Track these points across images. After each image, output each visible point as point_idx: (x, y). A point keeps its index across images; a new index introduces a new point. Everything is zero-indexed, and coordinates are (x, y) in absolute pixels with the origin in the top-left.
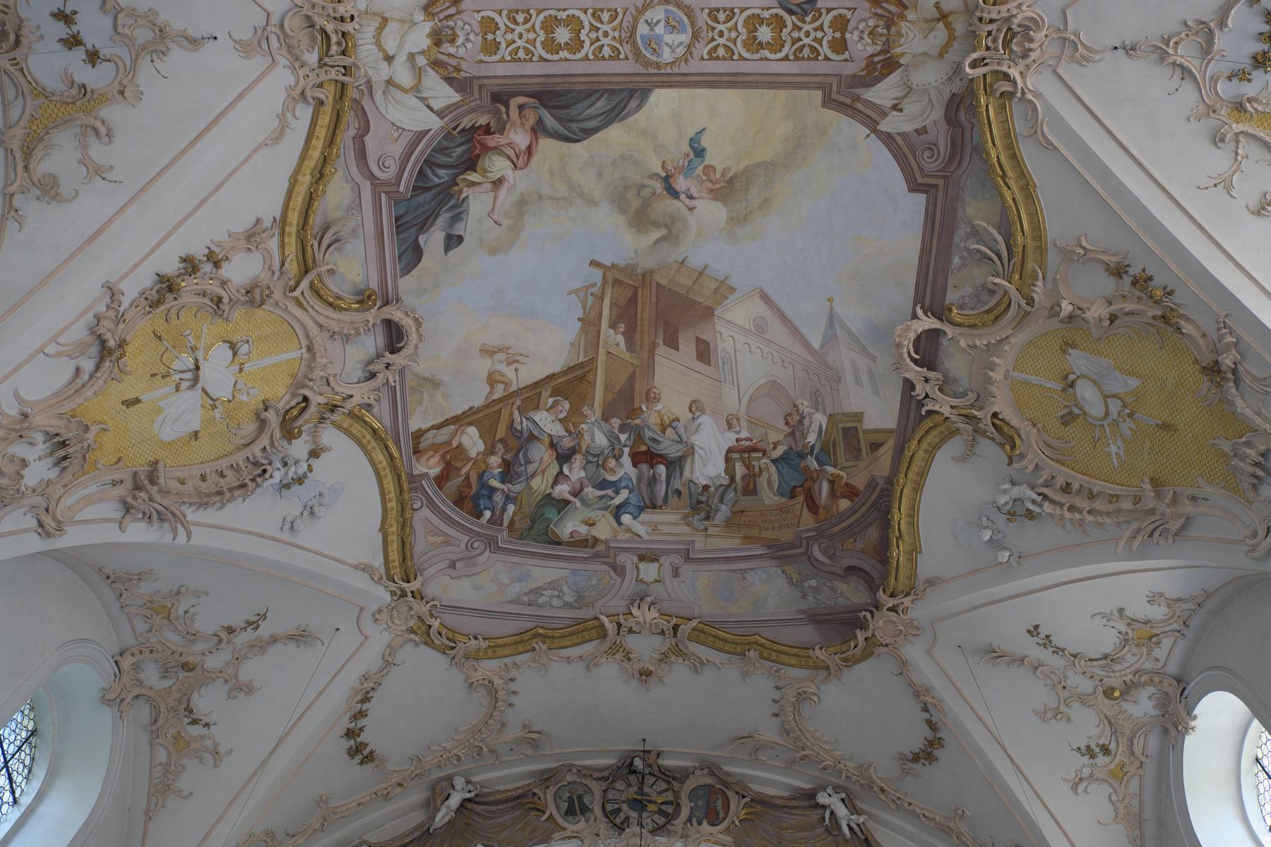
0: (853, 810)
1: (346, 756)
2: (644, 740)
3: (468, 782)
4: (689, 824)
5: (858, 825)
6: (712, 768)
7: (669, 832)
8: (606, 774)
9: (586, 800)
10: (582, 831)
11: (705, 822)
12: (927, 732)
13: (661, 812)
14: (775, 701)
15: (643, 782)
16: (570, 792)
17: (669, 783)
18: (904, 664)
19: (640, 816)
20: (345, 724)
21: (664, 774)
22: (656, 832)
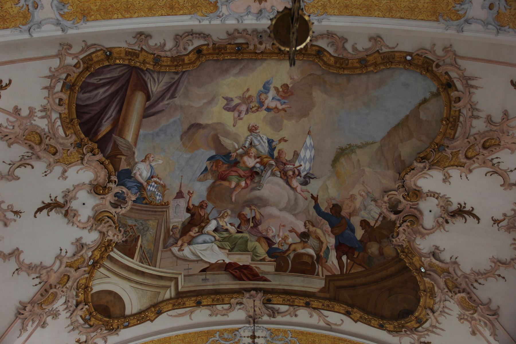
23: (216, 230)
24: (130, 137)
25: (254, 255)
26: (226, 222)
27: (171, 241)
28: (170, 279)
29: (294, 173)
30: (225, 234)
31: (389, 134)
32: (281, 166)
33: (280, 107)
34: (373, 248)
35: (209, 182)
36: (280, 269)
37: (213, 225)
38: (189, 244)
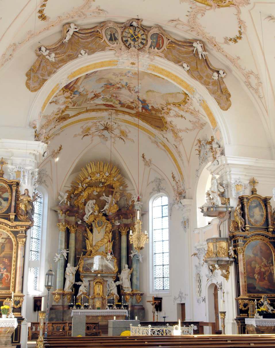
0: (204, 50)
1: (38, 19)
2: (138, 16)
3: (75, 25)
4: (150, 48)
5: (204, 55)
6: (159, 27)
7: (144, 50)
8: (122, 25)
9: (116, 35)
10: (116, 47)
11: (156, 48)
12: (238, 35)
13: (141, 43)
14: (189, 12)
15: (135, 31)
16: (111, 32)
17: (144, 31)
18: (239, 12)
19: (134, 43)
20: (39, 8)
21: (143, 28)
22: (140, 50)
23: (102, 98)
24: (79, 84)
25: (114, 103)
26: (107, 96)
27: (87, 101)
28: (85, 108)
29: (133, 90)
30: (106, 99)
31: (167, 94)
32: (129, 88)
33: (132, 76)
34: (153, 112)
35: (103, 88)
36: (121, 106)
37: (102, 97)
38: (93, 101)
